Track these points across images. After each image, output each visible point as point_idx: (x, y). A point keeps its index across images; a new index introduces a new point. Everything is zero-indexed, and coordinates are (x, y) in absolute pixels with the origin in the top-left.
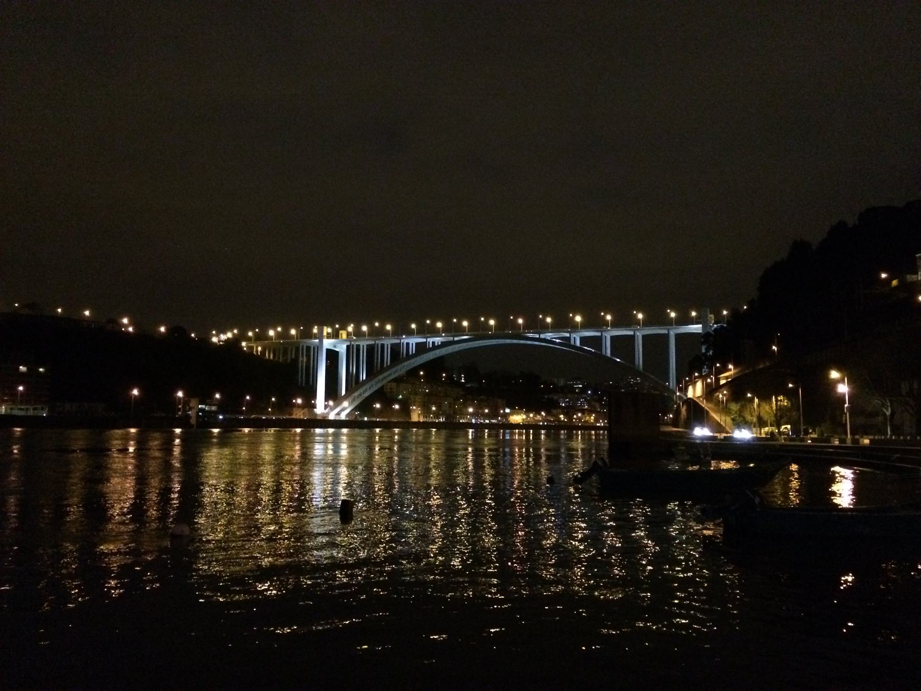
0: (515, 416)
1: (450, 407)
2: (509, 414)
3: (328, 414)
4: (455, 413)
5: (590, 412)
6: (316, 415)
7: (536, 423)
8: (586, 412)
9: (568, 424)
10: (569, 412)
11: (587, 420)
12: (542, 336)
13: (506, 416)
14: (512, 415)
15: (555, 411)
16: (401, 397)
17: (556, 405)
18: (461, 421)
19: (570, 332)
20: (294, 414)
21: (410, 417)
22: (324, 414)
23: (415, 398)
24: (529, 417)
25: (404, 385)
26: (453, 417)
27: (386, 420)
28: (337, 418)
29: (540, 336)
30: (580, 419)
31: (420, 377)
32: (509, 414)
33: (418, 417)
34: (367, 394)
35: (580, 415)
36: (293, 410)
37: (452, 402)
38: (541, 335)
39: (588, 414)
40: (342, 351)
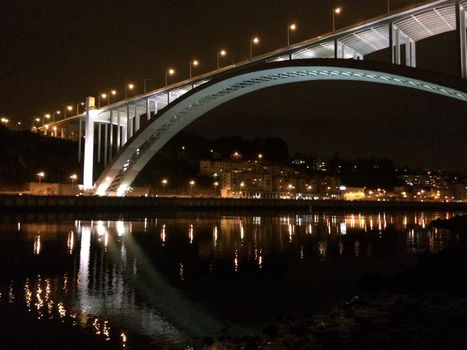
0: (351, 193)
1: (268, 184)
2: (345, 192)
3: (95, 190)
4: (275, 190)
5: (436, 190)
6: (82, 191)
7: (376, 199)
8: (432, 189)
9: (408, 200)
10: (410, 190)
11: (432, 197)
12: (294, 57)
13: (341, 193)
14: (348, 192)
15: (397, 189)
16: (216, 175)
17: (402, 184)
18: (281, 197)
19: (335, 40)
20: (31, 190)
21: (219, 193)
22: (91, 190)
23: (225, 176)
24: (369, 195)
25: (219, 163)
26: (271, 194)
27: (190, 197)
28: (111, 194)
29: (290, 57)
30: (422, 195)
31: (257, 159)
32: (345, 192)
33: (227, 193)
34: (139, 167)
35: (422, 191)
36: (29, 185)
37: (271, 179)
38: (293, 56)
39: (434, 191)
40: (124, 125)
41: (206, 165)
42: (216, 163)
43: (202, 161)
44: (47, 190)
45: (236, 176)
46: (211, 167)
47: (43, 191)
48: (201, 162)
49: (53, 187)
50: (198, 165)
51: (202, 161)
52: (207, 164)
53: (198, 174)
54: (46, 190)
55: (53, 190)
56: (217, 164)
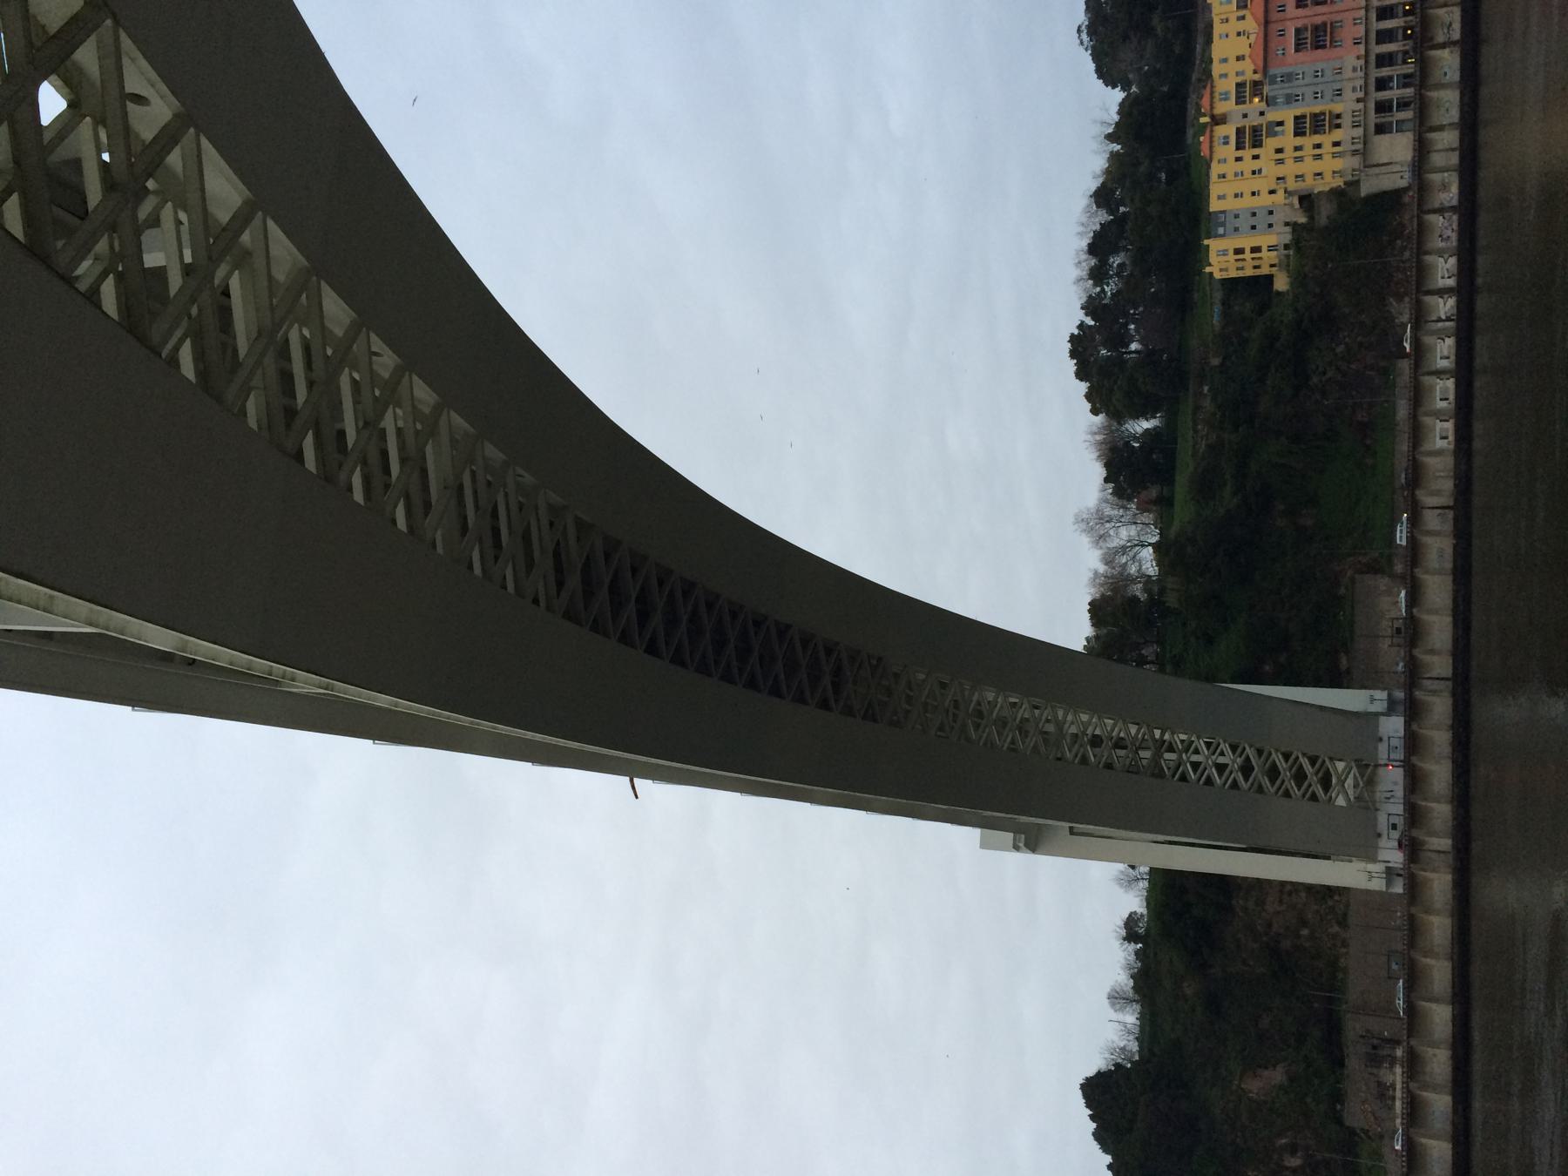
25: (1215, 189)
41: (1232, 257)
42: (1215, 205)
43: (1208, 269)
44: (1379, 1067)
45: (1281, 124)
46: (1236, 229)
47: (1379, 1084)
48: (1217, 275)
49: (1362, 1037)
50: (1232, 286)
51: (1208, 269)
52: (1225, 253)
53: (1281, 283)
54: (1375, 1071)
55: (1375, 1042)
56: (1219, 198)
